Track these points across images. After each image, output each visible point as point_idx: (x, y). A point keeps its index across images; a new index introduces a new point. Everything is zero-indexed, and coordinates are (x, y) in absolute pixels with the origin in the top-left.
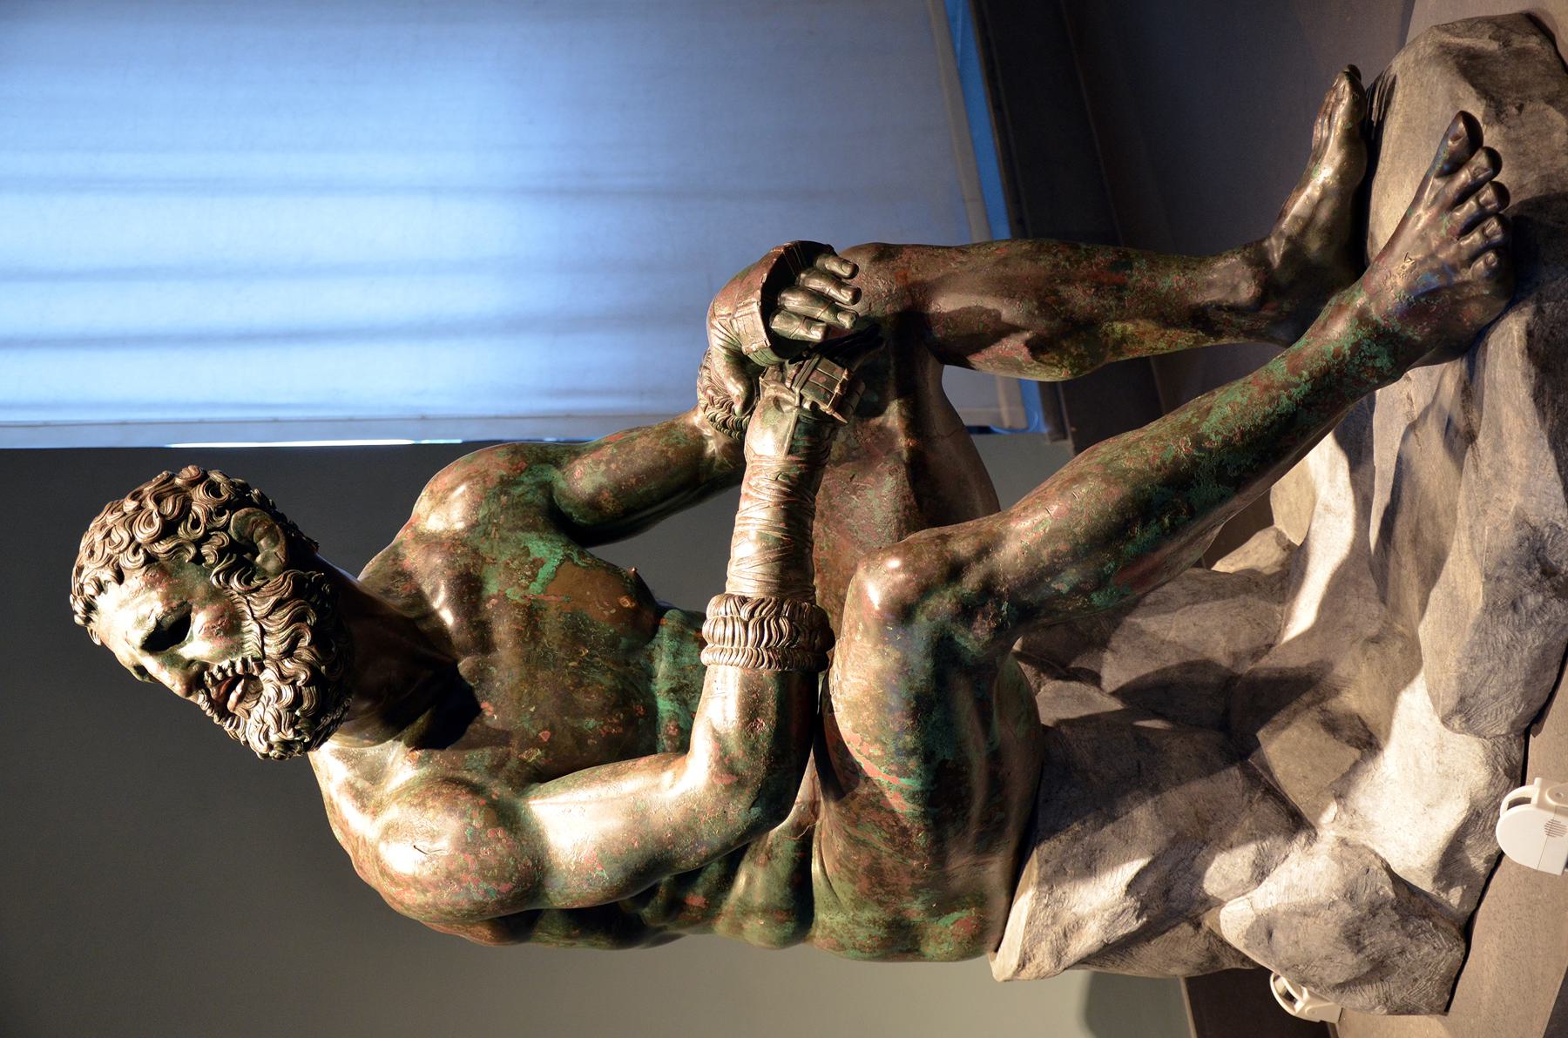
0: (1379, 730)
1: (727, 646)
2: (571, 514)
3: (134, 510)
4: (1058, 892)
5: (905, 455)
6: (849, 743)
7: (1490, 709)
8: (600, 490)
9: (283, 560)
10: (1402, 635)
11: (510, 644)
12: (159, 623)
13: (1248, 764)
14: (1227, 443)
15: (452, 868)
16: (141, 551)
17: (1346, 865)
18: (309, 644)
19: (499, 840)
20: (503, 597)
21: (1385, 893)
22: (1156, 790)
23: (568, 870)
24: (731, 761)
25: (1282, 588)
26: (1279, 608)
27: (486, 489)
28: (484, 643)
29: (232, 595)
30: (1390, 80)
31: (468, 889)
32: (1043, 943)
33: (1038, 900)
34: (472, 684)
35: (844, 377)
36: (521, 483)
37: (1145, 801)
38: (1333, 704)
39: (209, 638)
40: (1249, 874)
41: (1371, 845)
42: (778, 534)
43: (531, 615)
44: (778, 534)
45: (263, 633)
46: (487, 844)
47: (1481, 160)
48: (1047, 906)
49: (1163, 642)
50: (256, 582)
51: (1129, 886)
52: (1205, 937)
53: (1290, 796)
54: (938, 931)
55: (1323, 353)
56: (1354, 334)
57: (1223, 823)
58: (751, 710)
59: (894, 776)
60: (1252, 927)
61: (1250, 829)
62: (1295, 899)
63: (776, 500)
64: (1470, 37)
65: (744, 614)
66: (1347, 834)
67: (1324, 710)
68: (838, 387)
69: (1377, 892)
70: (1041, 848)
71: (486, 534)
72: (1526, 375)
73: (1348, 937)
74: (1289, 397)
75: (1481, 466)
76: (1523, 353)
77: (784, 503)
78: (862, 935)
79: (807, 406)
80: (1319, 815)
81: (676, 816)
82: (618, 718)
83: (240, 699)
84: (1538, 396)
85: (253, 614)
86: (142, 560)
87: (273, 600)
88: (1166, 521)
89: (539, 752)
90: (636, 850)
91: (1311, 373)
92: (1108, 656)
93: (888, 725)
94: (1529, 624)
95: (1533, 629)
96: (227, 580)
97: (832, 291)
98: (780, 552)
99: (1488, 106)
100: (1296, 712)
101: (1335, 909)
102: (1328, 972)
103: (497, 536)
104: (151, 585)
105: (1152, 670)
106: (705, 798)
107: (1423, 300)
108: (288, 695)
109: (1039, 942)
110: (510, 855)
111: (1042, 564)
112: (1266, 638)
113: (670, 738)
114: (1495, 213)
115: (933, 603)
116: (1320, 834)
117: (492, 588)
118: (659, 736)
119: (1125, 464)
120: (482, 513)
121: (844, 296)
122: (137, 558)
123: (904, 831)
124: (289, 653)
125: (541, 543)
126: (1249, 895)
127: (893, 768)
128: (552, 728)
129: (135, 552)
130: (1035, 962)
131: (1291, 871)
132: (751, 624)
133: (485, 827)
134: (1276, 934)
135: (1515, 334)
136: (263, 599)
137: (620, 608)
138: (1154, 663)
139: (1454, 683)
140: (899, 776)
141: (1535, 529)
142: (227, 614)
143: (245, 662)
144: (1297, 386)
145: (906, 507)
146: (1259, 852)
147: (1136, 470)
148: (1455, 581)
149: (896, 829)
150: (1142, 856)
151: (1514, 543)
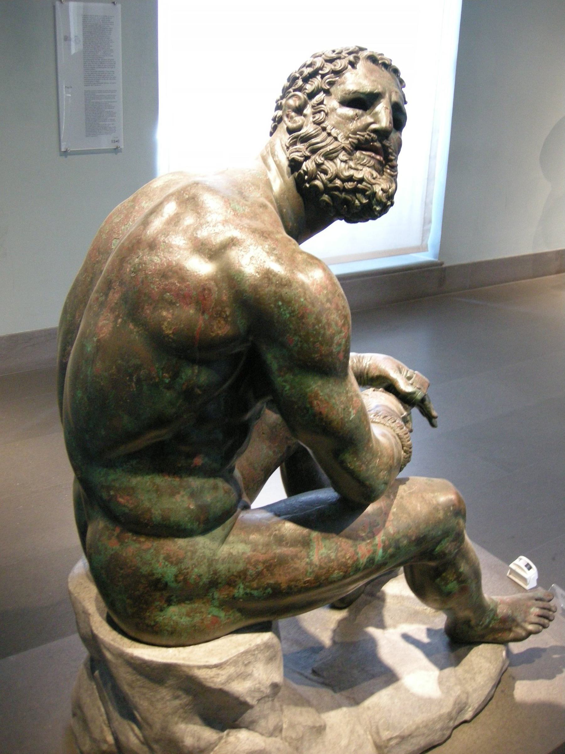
23: (347, 392)
31: (340, 332)
54: (203, 610)
59: (382, 545)
83: (379, 162)
93: (410, 529)
127: (387, 543)
149: (344, 560)
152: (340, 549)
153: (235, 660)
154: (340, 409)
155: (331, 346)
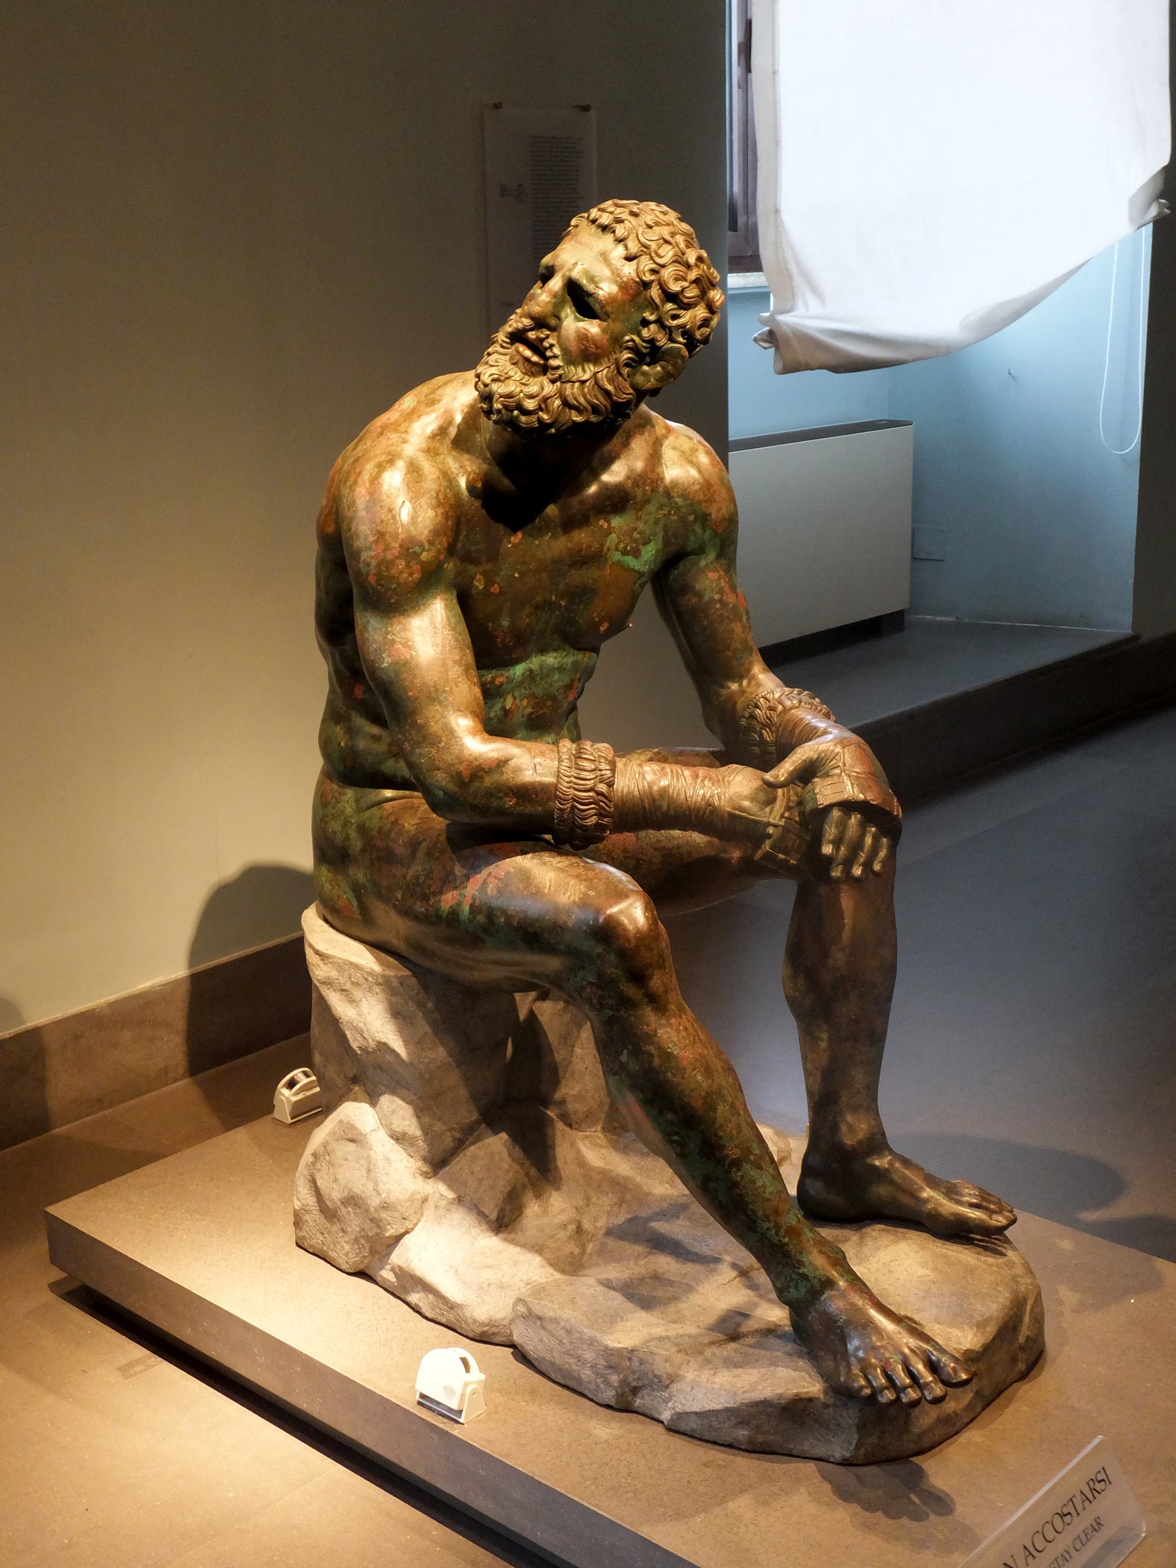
0: (510, 1233)
1: (574, 772)
2: (678, 569)
3: (687, 261)
4: (377, 989)
5: (723, 855)
6: (497, 866)
7: (532, 1334)
8: (700, 595)
9: (644, 388)
10: (583, 1252)
11: (570, 545)
12: (590, 295)
13: (481, 1125)
14: (735, 1184)
15: (388, 537)
16: (653, 277)
17: (408, 1204)
18: (573, 421)
19: (411, 575)
20: (609, 532)
21: (389, 1230)
22: (460, 1064)
23: (388, 633)
24: (482, 777)
25: (615, 1128)
26: (599, 1128)
27: (700, 502)
28: (570, 524)
29: (615, 353)
30: (1004, 1250)
31: (370, 549)
32: (336, 973)
33: (371, 974)
34: (537, 521)
35: (792, 861)
36: (704, 530)
37: (451, 1056)
38: (529, 1194)
39: (579, 337)
40: (397, 1130)
41: (423, 1219)
42: (665, 808)
43: (594, 558)
44: (665, 808)
45: (583, 382)
46: (408, 566)
47: (938, 1390)
48: (366, 980)
49: (573, 1046)
50: (626, 371)
51: (385, 1044)
52: (346, 1085)
53: (458, 1159)
55: (801, 1253)
56: (814, 1277)
57: (436, 1110)
58: (526, 793)
59: (471, 902)
60: (356, 1129)
61: (432, 1131)
62: (381, 1164)
63: (692, 808)
64: (1030, 1320)
65: (602, 788)
66: (431, 1202)
67: (524, 1187)
68: (783, 857)
69: (389, 1224)
70: (414, 979)
71: (661, 507)
72: (780, 1396)
73: (353, 1198)
74: (768, 1229)
75: (712, 1346)
76: (797, 1395)
77: (690, 813)
78: (335, 826)
79: (771, 830)
80: (445, 1182)
81: (435, 727)
82: (510, 642)
83: (527, 360)
84: (765, 1403)
85: (598, 372)
86: (644, 278)
87: (610, 387)
88: (676, 1138)
89: (481, 587)
90: (406, 693)
91: (786, 1244)
92: (561, 1005)
94: (597, 1374)
95: (593, 1376)
96: (627, 348)
97: (863, 857)
98: (651, 812)
99: (978, 1353)
100: (522, 1165)
101: (374, 1193)
102: (325, 1176)
103: (659, 516)
104: (623, 287)
105: (551, 1040)
106: (451, 754)
107: (839, 1331)
108: (530, 404)
109: (337, 970)
110: (399, 585)
111: (642, 1044)
112: (576, 1123)
113: (493, 679)
114: (898, 1399)
115: (612, 958)
116: (429, 1181)
117: (617, 522)
118: (494, 671)
119: (720, 1108)
120: (679, 501)
121: (857, 871)
122: (647, 275)
123: (425, 898)
124: (566, 403)
125: (653, 552)
126: (381, 1127)
127: (477, 903)
128: (501, 593)
129: (653, 271)
130: (321, 963)
131: (401, 1161)
132: (591, 794)
133: (422, 563)
134: (352, 1146)
135: (812, 1389)
136: (611, 380)
137: (600, 623)
138: (556, 1042)
139: (552, 1314)
140: (471, 906)
141: (667, 1387)
142: (599, 351)
143: (558, 368)
144: (777, 1234)
145: (682, 855)
146: (414, 1137)
147: (715, 1118)
148: (627, 1320)
149: (428, 891)
150: (408, 1054)
151: (656, 1372)
152: (431, 876)
153: (339, 963)
154: (371, 648)
155: (358, 562)
